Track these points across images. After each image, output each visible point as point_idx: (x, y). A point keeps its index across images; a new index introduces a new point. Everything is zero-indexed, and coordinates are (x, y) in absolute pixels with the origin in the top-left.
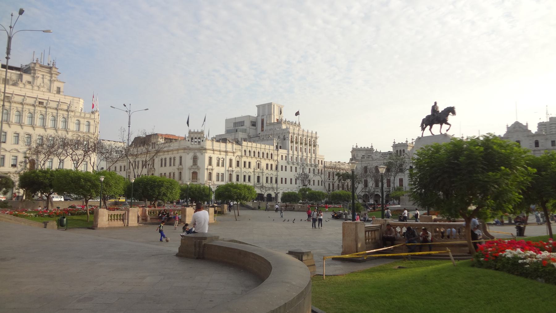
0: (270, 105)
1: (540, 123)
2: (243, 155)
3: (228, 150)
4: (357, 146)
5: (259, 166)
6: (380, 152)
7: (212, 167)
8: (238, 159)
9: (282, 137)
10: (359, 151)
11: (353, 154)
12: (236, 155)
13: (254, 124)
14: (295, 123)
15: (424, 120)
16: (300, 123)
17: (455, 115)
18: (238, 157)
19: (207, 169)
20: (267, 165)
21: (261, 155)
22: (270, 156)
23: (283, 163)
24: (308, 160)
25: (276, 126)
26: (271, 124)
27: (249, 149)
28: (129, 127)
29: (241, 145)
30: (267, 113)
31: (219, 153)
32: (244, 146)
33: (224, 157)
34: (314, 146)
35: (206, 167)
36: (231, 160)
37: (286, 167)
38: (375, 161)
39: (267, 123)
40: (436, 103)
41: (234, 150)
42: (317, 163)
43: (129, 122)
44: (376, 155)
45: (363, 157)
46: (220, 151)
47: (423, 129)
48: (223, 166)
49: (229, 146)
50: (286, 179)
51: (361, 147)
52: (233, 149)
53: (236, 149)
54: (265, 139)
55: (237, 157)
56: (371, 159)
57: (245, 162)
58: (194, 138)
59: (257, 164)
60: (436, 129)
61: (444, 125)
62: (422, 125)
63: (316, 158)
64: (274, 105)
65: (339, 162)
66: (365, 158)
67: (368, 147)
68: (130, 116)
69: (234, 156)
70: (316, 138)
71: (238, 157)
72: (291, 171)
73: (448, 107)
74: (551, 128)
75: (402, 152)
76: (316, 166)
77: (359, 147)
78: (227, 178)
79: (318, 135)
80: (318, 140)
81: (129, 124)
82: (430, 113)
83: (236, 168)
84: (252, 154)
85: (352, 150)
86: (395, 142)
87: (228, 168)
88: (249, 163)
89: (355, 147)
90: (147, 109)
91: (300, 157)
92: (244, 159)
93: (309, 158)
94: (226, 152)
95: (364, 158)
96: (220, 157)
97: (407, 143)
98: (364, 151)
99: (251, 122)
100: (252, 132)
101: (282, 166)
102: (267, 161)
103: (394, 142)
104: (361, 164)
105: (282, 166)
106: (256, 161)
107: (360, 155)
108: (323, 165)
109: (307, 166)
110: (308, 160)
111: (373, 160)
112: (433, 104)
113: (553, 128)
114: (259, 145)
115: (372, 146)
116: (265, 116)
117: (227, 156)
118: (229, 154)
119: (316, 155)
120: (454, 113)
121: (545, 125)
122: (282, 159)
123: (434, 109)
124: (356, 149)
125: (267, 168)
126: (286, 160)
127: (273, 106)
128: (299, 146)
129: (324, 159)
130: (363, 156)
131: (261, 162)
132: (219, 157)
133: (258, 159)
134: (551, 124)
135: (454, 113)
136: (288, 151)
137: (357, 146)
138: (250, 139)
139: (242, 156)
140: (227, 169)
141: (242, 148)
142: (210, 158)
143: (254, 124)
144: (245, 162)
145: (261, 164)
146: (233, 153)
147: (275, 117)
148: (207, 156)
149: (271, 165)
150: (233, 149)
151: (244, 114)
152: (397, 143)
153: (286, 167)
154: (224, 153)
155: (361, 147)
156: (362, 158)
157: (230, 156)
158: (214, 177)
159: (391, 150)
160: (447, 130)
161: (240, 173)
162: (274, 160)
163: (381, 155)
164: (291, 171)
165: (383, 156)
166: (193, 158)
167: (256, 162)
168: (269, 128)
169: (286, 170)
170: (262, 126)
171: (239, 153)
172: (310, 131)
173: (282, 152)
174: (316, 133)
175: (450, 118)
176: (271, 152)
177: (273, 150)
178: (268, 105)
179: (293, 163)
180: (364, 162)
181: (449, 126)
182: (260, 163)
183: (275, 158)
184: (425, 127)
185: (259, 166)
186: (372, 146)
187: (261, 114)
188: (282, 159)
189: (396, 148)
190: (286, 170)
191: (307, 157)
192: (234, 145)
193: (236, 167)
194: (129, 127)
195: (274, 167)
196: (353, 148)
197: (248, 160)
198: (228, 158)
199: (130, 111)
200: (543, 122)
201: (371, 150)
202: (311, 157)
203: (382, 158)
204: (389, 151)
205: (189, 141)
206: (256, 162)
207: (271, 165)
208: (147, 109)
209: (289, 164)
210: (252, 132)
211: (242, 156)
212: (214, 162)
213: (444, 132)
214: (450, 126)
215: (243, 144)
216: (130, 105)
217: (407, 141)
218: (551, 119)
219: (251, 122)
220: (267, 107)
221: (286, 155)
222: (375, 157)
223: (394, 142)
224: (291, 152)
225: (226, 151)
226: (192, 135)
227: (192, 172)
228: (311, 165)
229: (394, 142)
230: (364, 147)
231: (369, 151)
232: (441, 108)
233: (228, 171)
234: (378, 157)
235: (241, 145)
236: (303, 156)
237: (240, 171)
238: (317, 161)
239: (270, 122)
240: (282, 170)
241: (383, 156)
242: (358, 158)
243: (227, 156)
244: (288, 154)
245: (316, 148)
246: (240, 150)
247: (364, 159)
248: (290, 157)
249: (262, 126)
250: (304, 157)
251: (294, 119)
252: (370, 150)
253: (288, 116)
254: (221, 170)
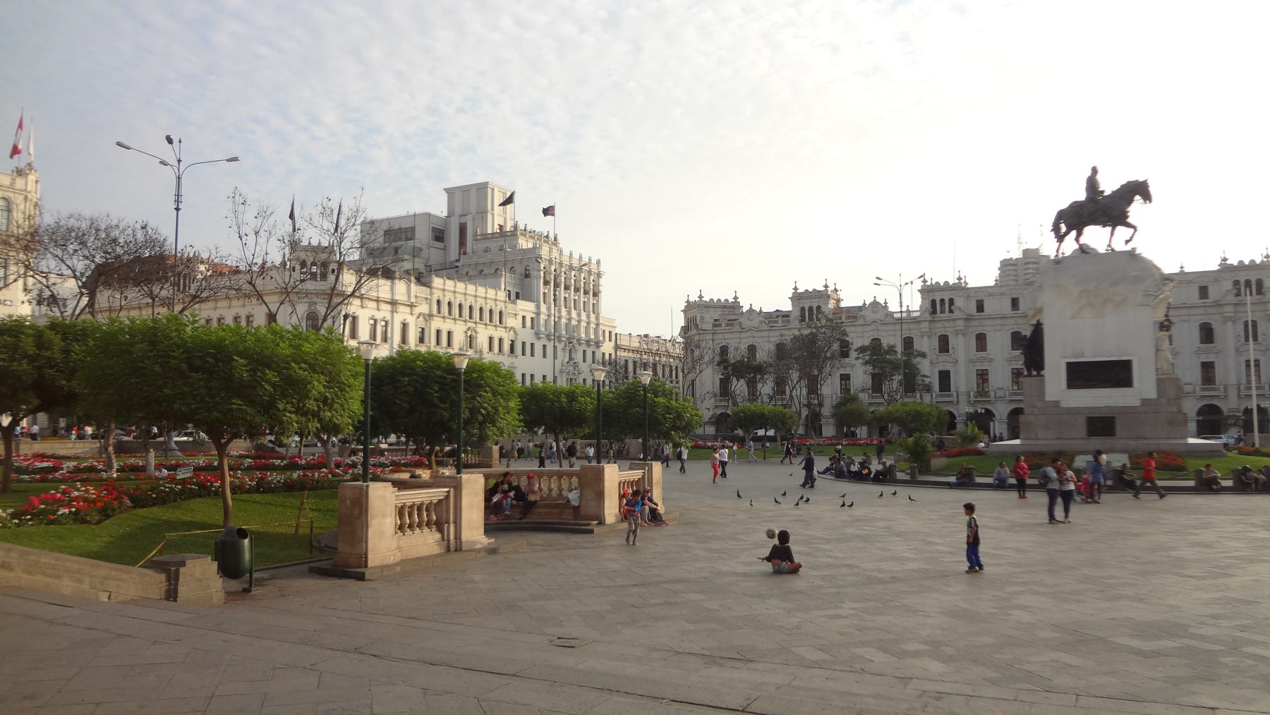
0: (482, 189)
1: (1005, 260)
2: (435, 312)
3: (397, 297)
4: (701, 297)
5: (471, 341)
6: (761, 311)
9: (520, 269)
10: (707, 309)
11: (689, 316)
12: (417, 311)
13: (439, 236)
14: (547, 237)
15: (1062, 216)
16: (559, 238)
17: (1150, 202)
18: (421, 318)
20: (491, 339)
21: (476, 314)
22: (496, 317)
23: (526, 335)
24: (583, 329)
25: (494, 245)
26: (485, 237)
27: (449, 296)
28: (177, 209)
29: (428, 285)
30: (473, 210)
32: (436, 288)
33: (388, 318)
34: (595, 295)
36: (405, 326)
37: (532, 345)
38: (749, 334)
39: (475, 235)
40: (1095, 171)
41: (413, 300)
42: (601, 338)
43: (178, 195)
44: (749, 319)
45: (716, 323)
46: (378, 301)
47: (1060, 238)
49: (400, 286)
50: (532, 376)
51: (712, 300)
52: (409, 297)
53: (416, 296)
54: (486, 271)
56: (737, 328)
57: (438, 332)
59: (466, 336)
60: (1096, 237)
61: (1120, 229)
62: (1056, 228)
63: (597, 325)
64: (493, 189)
65: (646, 336)
66: (723, 325)
67: (726, 300)
68: (179, 178)
69: (411, 314)
70: (599, 275)
71: (421, 318)
72: (544, 356)
73: (1129, 182)
74: (1027, 271)
75: (815, 312)
76: (598, 344)
77: (706, 299)
79: (602, 269)
80: (602, 281)
81: (178, 201)
82: (1081, 196)
84: (456, 311)
85: (686, 307)
86: (798, 287)
88: (449, 333)
89: (694, 298)
90: (235, 159)
91: (564, 321)
92: (437, 323)
93: (583, 324)
94: (393, 303)
95: (720, 325)
96: (379, 315)
97: (827, 291)
98: (718, 310)
99: (434, 230)
100: (435, 256)
101: (524, 343)
102: (491, 331)
103: (796, 289)
104: (1266, 311)
105: (524, 343)
106: (465, 328)
107: (710, 317)
108: (613, 344)
109: (580, 344)
110: (583, 329)
111: (742, 330)
112: (1089, 173)
113: (1031, 271)
114: (471, 288)
115: (736, 298)
116: (469, 217)
117: (395, 314)
118: (401, 308)
119: (597, 318)
120: (1147, 197)
121: (1015, 265)
122: (524, 326)
123: (1092, 184)
124: (701, 302)
125: (491, 349)
126: (532, 328)
127: (489, 190)
128: (562, 293)
129: (615, 327)
130: (716, 320)
131: (476, 332)
132: (376, 317)
133: (469, 324)
134: (1028, 263)
135: (1147, 197)
136: (538, 307)
137: (701, 297)
138: (451, 270)
139: (431, 315)
141: (431, 294)
143: (439, 236)
144: (438, 332)
145: (476, 338)
146: (411, 306)
147: (497, 219)
149: (501, 340)
150: (409, 297)
151: (419, 209)
152: (801, 290)
153: (532, 345)
154: (388, 307)
155: (712, 300)
156: (714, 326)
157: (403, 314)
159: (787, 306)
160: (1127, 242)
162: (505, 328)
163: (761, 319)
164: (544, 356)
165: (767, 322)
166: (305, 317)
167: (465, 332)
168: (482, 246)
169: (532, 355)
170: (462, 243)
171: (423, 308)
172: (576, 256)
173: (526, 307)
174: (598, 262)
175: (1136, 210)
176: (501, 306)
177: (505, 302)
178: (478, 189)
179: (548, 337)
180: (720, 336)
181: (1132, 230)
182: (474, 334)
183: (510, 322)
184: (1067, 233)
185: (471, 341)
186: (736, 298)
187: (458, 211)
188: (524, 326)
189: (801, 302)
190: (532, 355)
191: (579, 321)
192: (413, 286)
193: (418, 343)
194: (177, 209)
195: (506, 347)
196: (688, 302)
197: (445, 326)
198: (398, 319)
199: (179, 161)
200: (1011, 259)
201: (734, 306)
202: (588, 323)
203: (766, 327)
204: (777, 311)
207: (501, 340)
208: (235, 159)
209: (539, 338)
210: (435, 256)
211: (431, 315)
213: (1119, 246)
214: (1136, 230)
215: (434, 285)
216: (180, 142)
217: (826, 286)
218: (1026, 252)
219: (434, 230)
220: (473, 193)
221: (533, 316)
222: (747, 324)
223: (796, 287)
224: (543, 308)
225: (393, 300)
226: (303, 256)
228: (588, 342)
229: (796, 287)
230: (719, 300)
231: (729, 312)
232: (1109, 185)
234: (755, 323)
235: (428, 285)
236: (570, 319)
238: (601, 332)
239: (484, 233)
240: (523, 354)
241: (767, 322)
242: (705, 326)
243: (395, 314)
244: (538, 314)
245: (598, 301)
246: (426, 298)
247: (720, 328)
248: (542, 322)
249: (462, 243)
250: (574, 323)
251: (542, 225)
252: (731, 307)
253: (526, 215)
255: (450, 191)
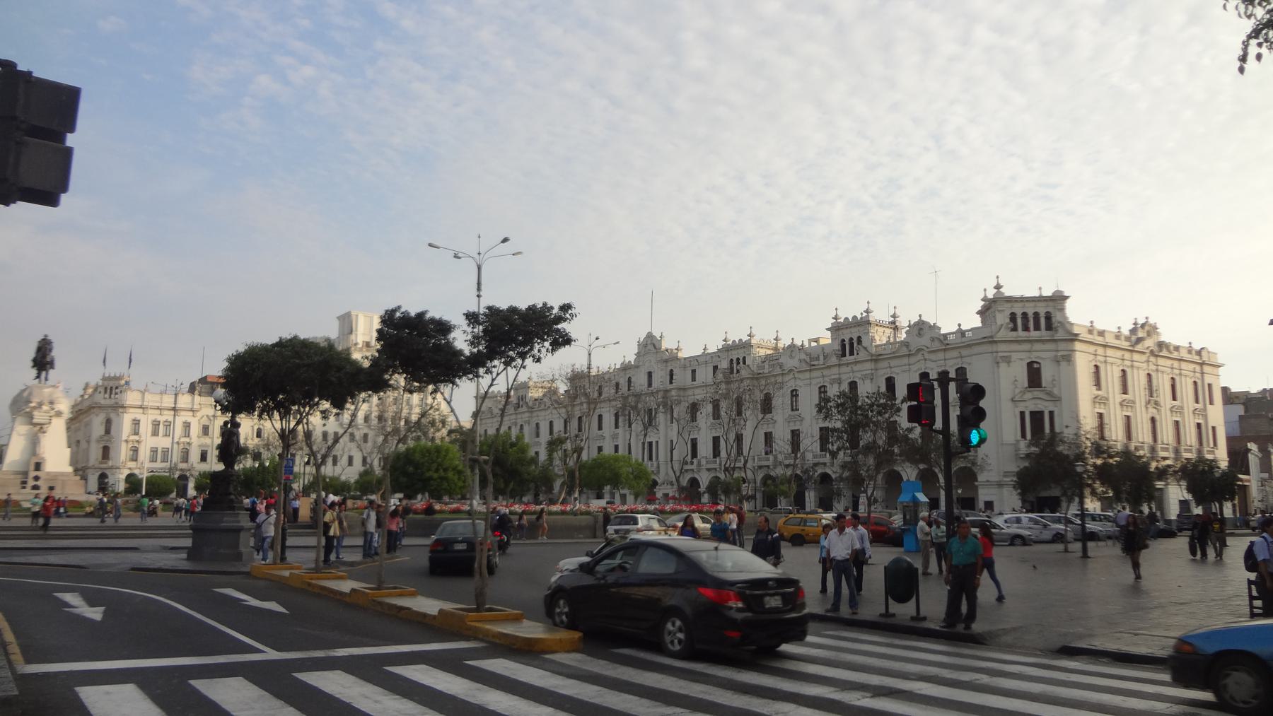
7: (140, 437)
8: (205, 421)
12: (199, 414)
19: (127, 441)
31: (158, 412)
33: (171, 419)
35: (124, 437)
41: (196, 407)
46: (158, 408)
48: (166, 435)
55: (202, 418)
58: (114, 388)
59: (253, 429)
71: (205, 418)
78: (176, 457)
83: (198, 437)
87: (180, 439)
96: (162, 419)
131: (263, 425)
132: (158, 420)
139: (214, 416)
140: (176, 440)
142: (136, 423)
146: (192, 410)
148: (127, 419)
154: (172, 413)
158: (144, 454)
161: (210, 448)
167: (253, 427)
182: (261, 427)
205: (100, 392)
206: (253, 427)
212: (145, 428)
226: (106, 383)
227: (102, 445)
233: (178, 443)
237: (210, 445)
254: (163, 442)
255: (338, 318)
